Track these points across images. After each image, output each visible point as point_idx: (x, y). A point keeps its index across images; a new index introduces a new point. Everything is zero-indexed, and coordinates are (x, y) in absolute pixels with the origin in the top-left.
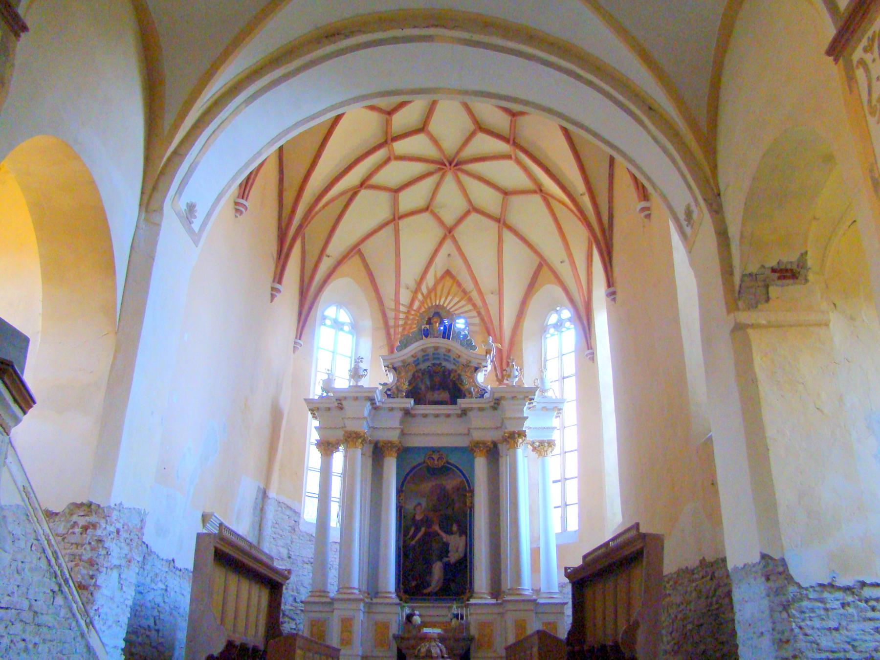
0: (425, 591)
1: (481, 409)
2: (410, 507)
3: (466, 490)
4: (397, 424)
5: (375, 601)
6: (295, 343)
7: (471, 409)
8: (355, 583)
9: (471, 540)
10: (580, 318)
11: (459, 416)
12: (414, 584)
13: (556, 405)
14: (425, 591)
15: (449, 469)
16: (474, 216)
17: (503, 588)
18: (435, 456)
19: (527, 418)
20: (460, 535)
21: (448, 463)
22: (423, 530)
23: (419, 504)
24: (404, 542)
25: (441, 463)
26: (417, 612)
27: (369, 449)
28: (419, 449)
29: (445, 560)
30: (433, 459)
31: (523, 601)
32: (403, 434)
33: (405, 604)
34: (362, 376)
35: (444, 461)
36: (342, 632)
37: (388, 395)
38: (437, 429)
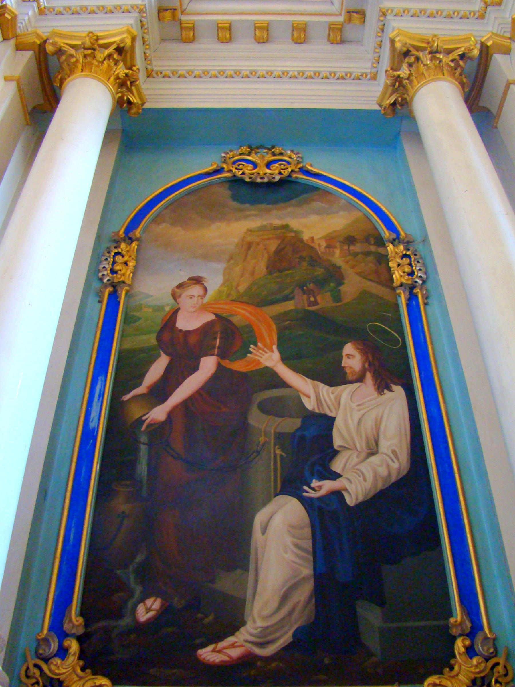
3: (380, 242)
12: (147, 610)
20: (382, 386)
22: (208, 365)
24: (117, 409)
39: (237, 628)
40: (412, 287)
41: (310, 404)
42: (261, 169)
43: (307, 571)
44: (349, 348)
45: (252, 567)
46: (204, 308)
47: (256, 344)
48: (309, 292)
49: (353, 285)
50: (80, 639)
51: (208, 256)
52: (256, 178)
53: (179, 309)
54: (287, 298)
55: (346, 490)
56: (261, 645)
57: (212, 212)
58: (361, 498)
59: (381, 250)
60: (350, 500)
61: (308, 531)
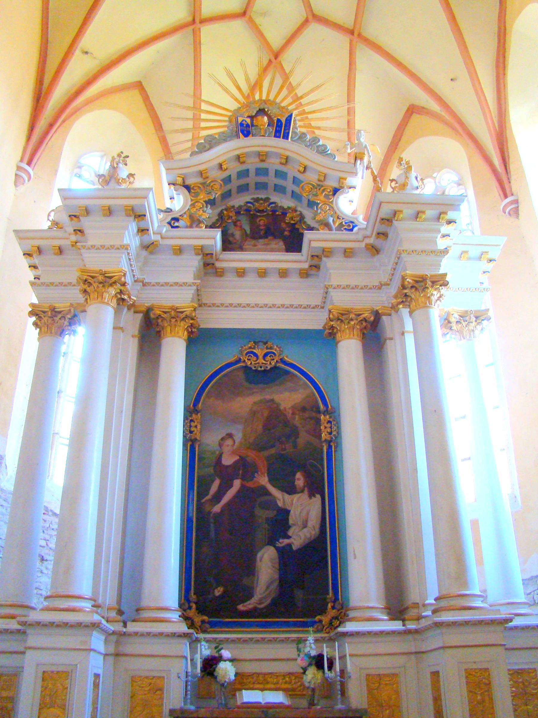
0: (241, 607)
1: (348, 253)
2: (211, 440)
3: (319, 412)
4: (189, 278)
5: (132, 627)
6: (19, 168)
7: (327, 253)
8: (85, 588)
11: (304, 274)
12: (218, 591)
13: (485, 249)
14: (241, 607)
15: (287, 373)
16: (314, 28)
18: (260, 352)
20: (311, 495)
22: (237, 484)
23: (230, 436)
26: (226, 653)
27: (133, 322)
30: (256, 355)
31: (480, 623)
33: (201, 636)
35: (276, 358)
38: (263, 297)
39: (251, 598)
40: (330, 441)
41: (280, 504)
43: (276, 576)
44: (299, 475)
45: (256, 574)
46: (234, 453)
47: (258, 473)
48: (282, 443)
49: (303, 438)
50: (196, 603)
51: (234, 421)
52: (258, 367)
53: (223, 453)
54: (272, 446)
55: (293, 543)
56: (259, 604)
57: (236, 391)
58: (298, 547)
59: (318, 416)
60: (294, 548)
61: (277, 560)
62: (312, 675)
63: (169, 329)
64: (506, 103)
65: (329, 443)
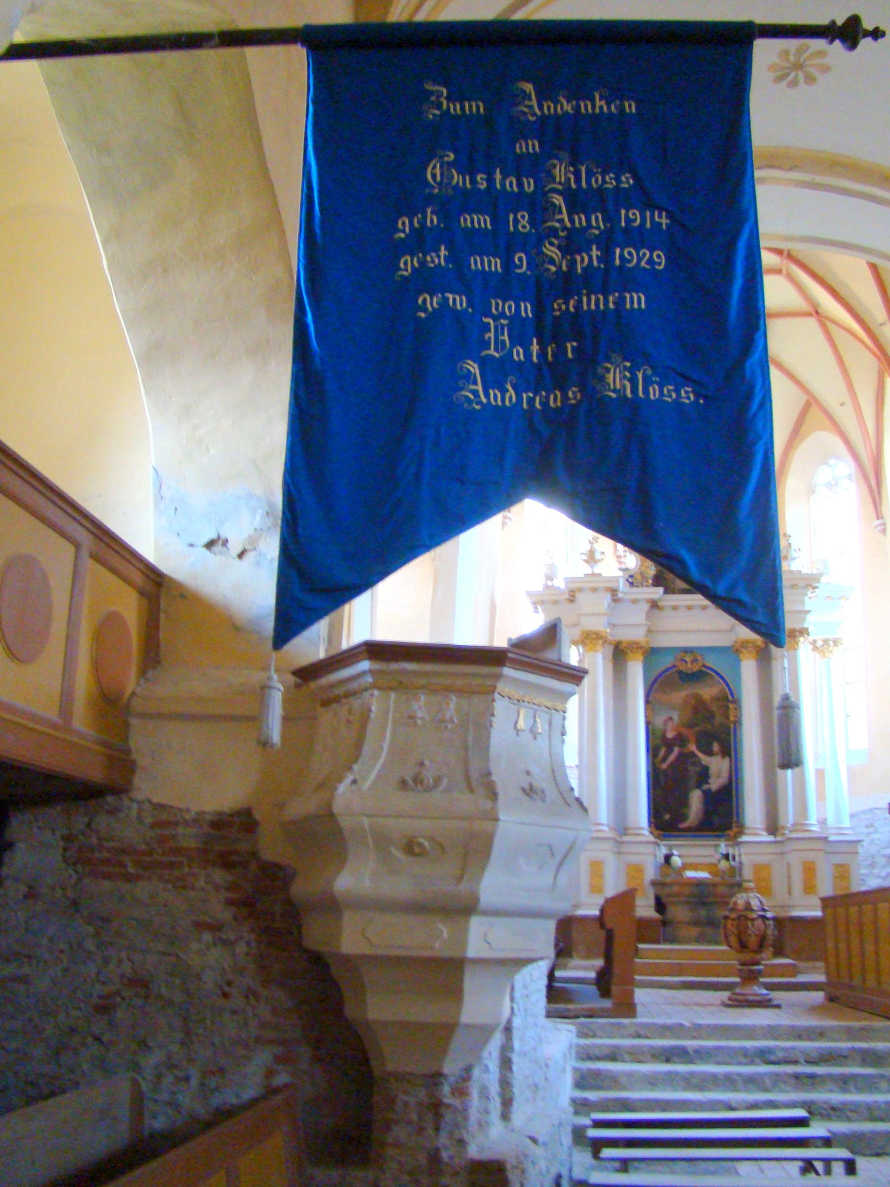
0: (681, 826)
2: (659, 721)
3: (728, 700)
9: (736, 761)
10: (865, 477)
12: (667, 817)
14: (681, 826)
15: (708, 673)
17: (782, 821)
18: (688, 659)
19: (810, 611)
21: (704, 666)
22: (676, 750)
23: (671, 718)
25: (695, 668)
26: (675, 852)
28: (667, 649)
29: (706, 787)
30: (686, 662)
32: (649, 631)
34: (599, 561)
35: (700, 664)
36: (591, 877)
37: (631, 584)
41: (703, 762)
42: (690, 667)
49: (718, 719)
62: (724, 864)
63: (631, 654)
64: (883, 434)
65: (735, 723)
